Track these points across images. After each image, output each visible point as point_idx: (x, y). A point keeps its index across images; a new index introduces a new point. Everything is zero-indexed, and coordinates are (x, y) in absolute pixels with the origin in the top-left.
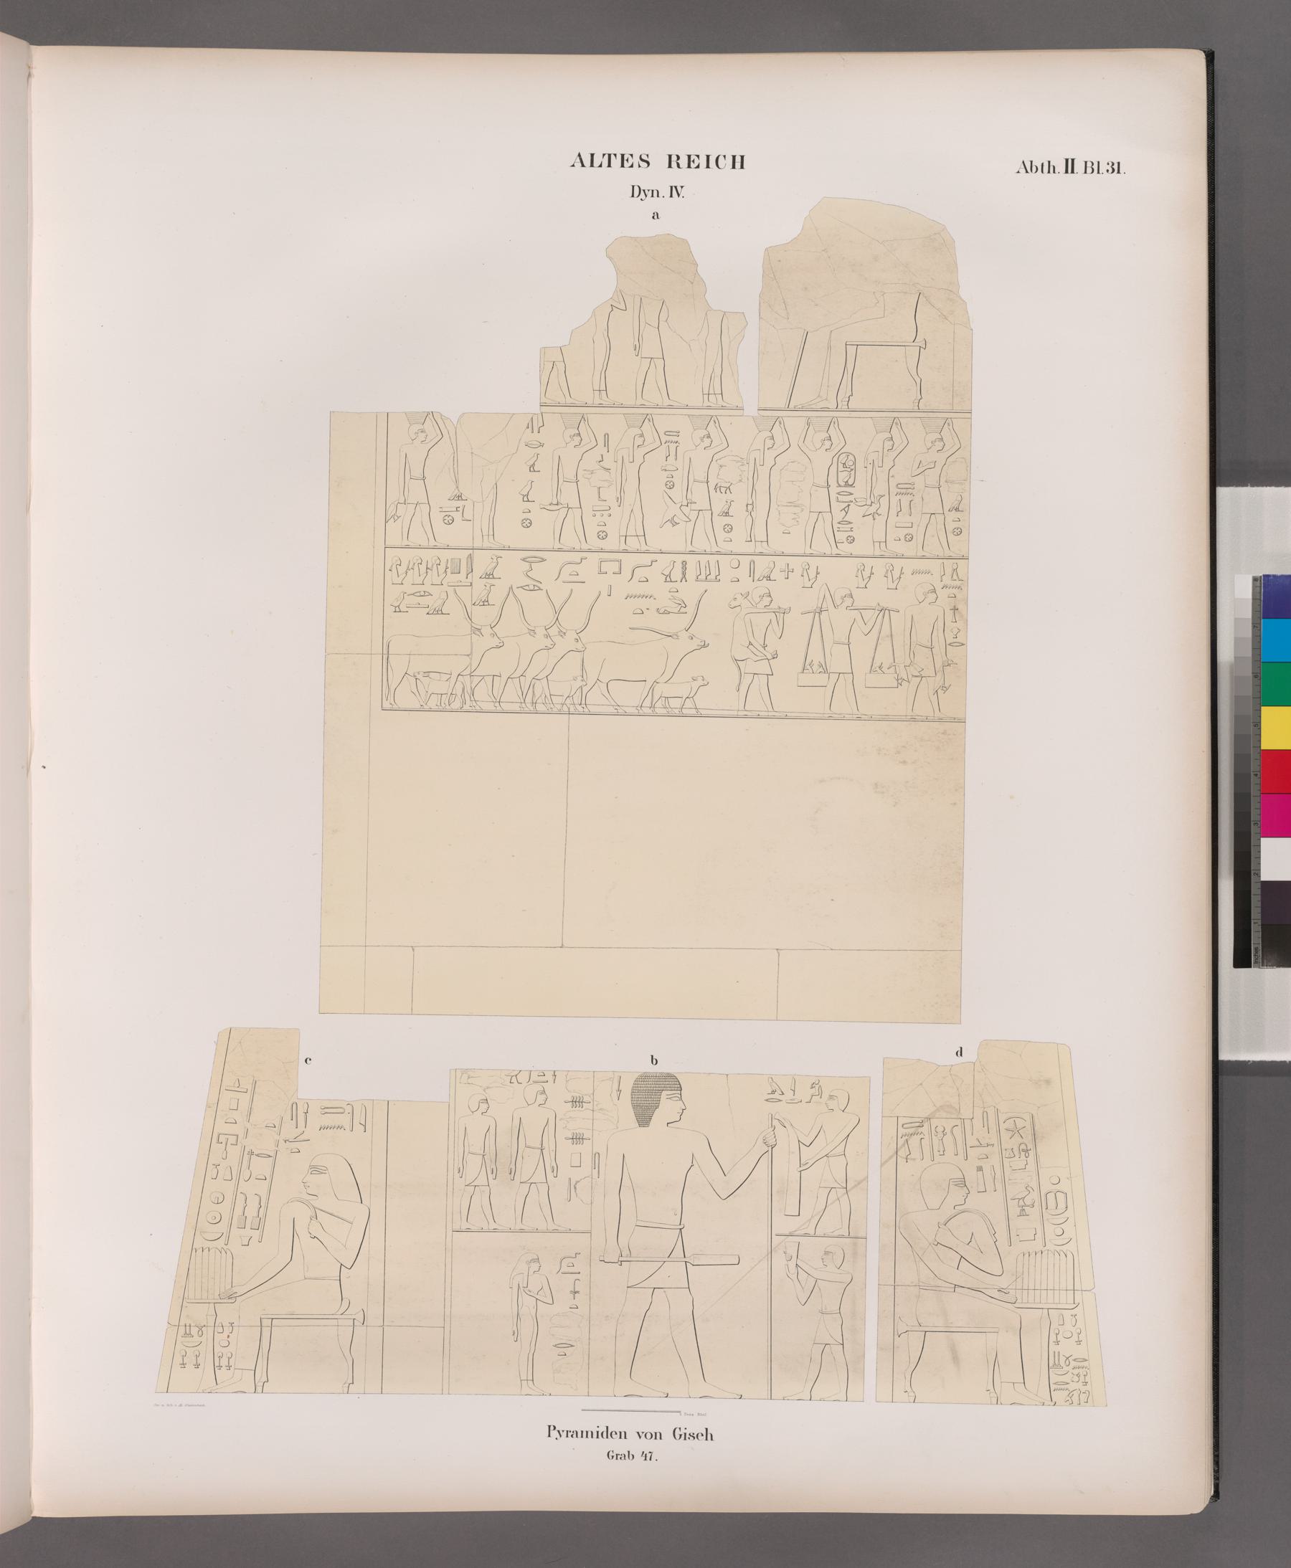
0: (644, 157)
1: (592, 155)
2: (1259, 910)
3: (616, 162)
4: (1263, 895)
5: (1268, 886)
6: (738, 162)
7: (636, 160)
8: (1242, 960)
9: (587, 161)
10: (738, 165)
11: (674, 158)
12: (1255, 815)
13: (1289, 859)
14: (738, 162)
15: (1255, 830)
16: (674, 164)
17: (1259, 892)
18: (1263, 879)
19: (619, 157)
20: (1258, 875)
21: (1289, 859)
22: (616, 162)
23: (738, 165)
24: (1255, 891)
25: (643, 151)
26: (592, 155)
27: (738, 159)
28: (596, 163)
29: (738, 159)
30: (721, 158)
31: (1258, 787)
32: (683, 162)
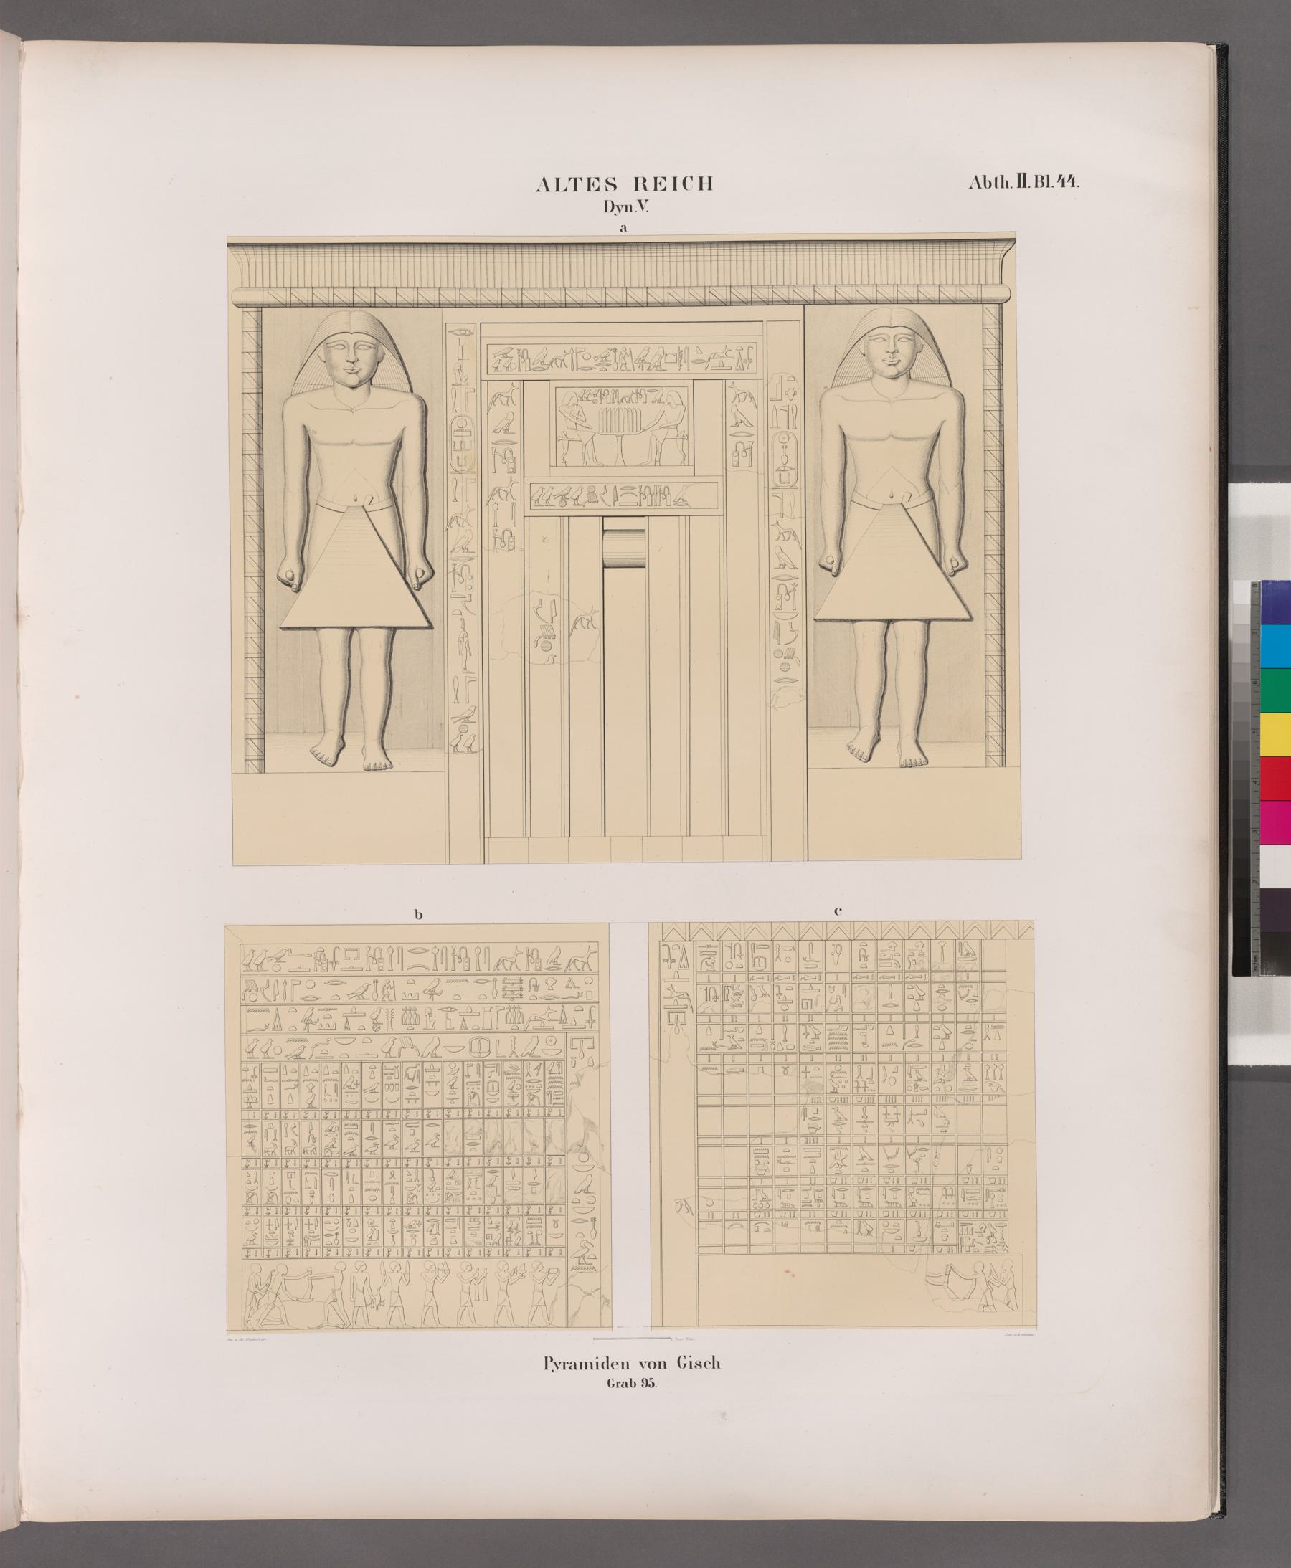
0: (611, 181)
1: (558, 180)
2: (1258, 918)
3: (582, 186)
4: (1262, 903)
5: (1269, 894)
6: (706, 183)
7: (603, 184)
8: (1242, 969)
9: (552, 186)
10: (705, 186)
11: (640, 181)
12: (1254, 822)
13: (1286, 867)
14: (706, 183)
15: (1254, 837)
16: (641, 187)
17: (1258, 900)
18: (1262, 886)
19: (585, 181)
20: (1258, 883)
21: (1286, 867)
22: (582, 186)
23: (705, 186)
24: (1255, 898)
25: (610, 176)
26: (558, 180)
27: (705, 181)
28: (562, 188)
29: (705, 181)
30: (688, 180)
31: (1257, 794)
32: (650, 184)
